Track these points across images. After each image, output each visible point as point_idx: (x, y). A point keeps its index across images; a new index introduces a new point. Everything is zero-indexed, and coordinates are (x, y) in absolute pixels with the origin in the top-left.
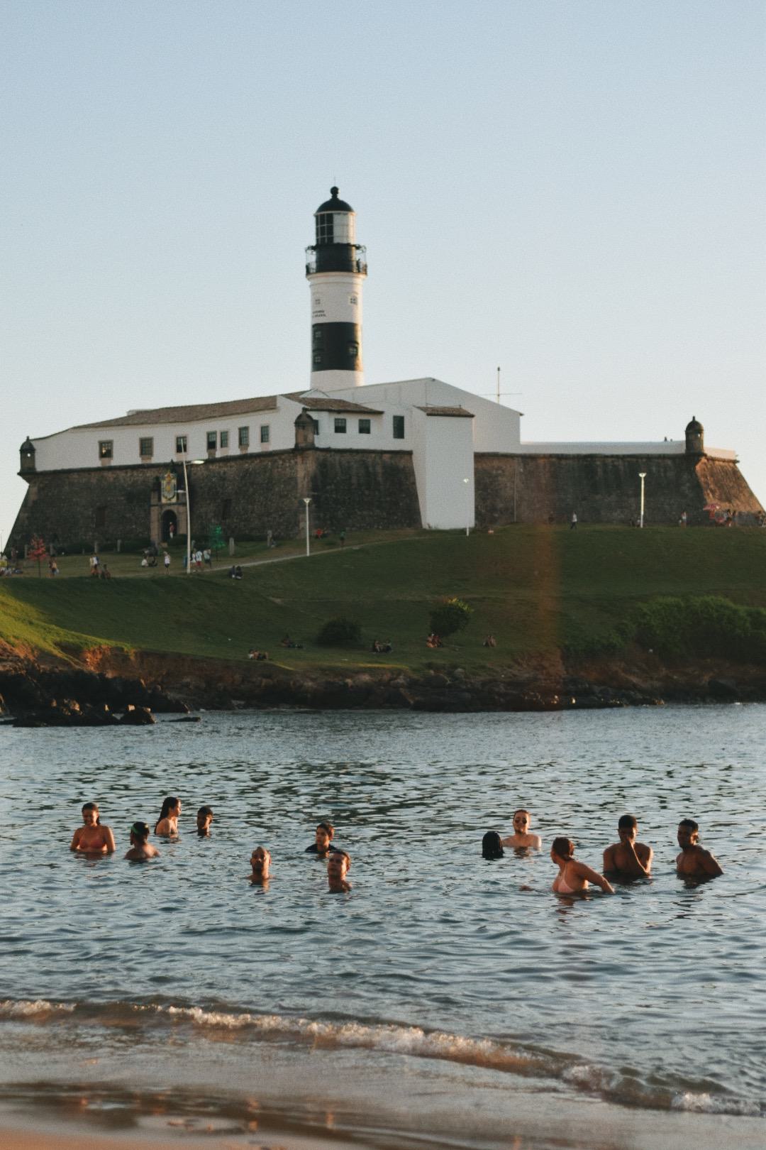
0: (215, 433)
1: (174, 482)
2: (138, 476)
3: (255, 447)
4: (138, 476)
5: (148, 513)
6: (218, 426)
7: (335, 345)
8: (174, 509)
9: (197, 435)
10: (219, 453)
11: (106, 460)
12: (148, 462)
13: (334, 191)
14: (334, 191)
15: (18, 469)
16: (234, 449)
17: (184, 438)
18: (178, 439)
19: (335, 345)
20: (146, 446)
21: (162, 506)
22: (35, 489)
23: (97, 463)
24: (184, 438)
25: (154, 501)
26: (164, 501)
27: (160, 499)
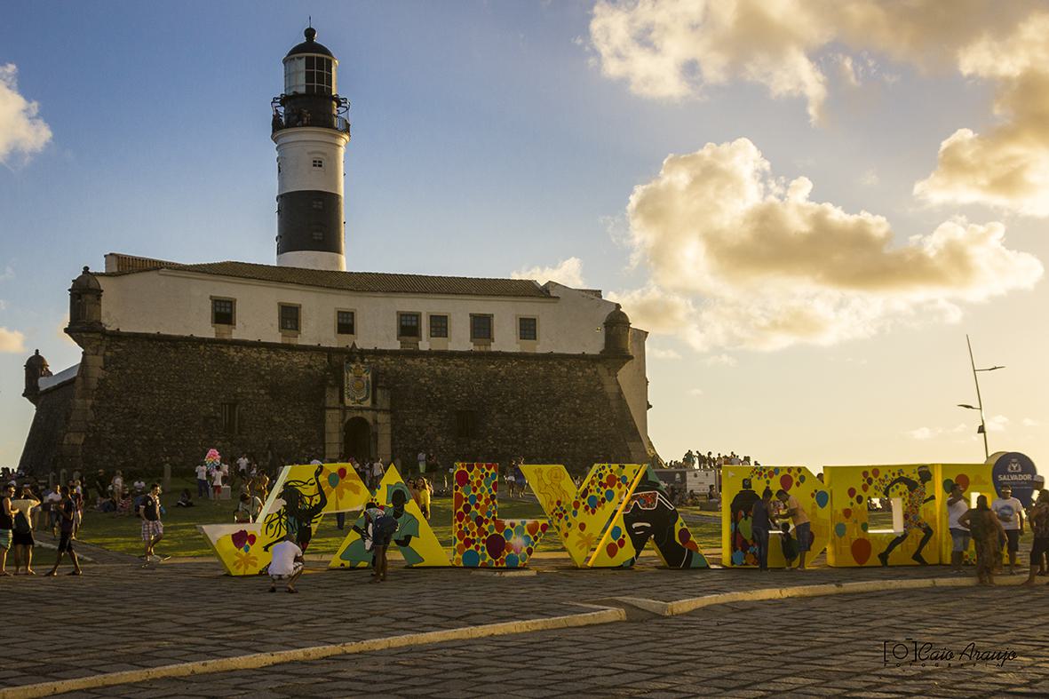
0: (417, 316)
1: (368, 376)
2: (281, 360)
3: (506, 339)
4: (281, 360)
5: (320, 421)
6: (425, 307)
7: (310, 218)
8: (368, 416)
9: (460, 313)
10: (424, 345)
11: (224, 327)
12: (294, 341)
13: (310, 33)
14: (310, 33)
15: (66, 320)
16: (460, 339)
17: (351, 314)
18: (341, 314)
19: (310, 218)
20: (290, 317)
21: (346, 409)
22: (99, 360)
23: (207, 330)
24: (351, 314)
25: (331, 399)
26: (349, 402)
27: (342, 400)
